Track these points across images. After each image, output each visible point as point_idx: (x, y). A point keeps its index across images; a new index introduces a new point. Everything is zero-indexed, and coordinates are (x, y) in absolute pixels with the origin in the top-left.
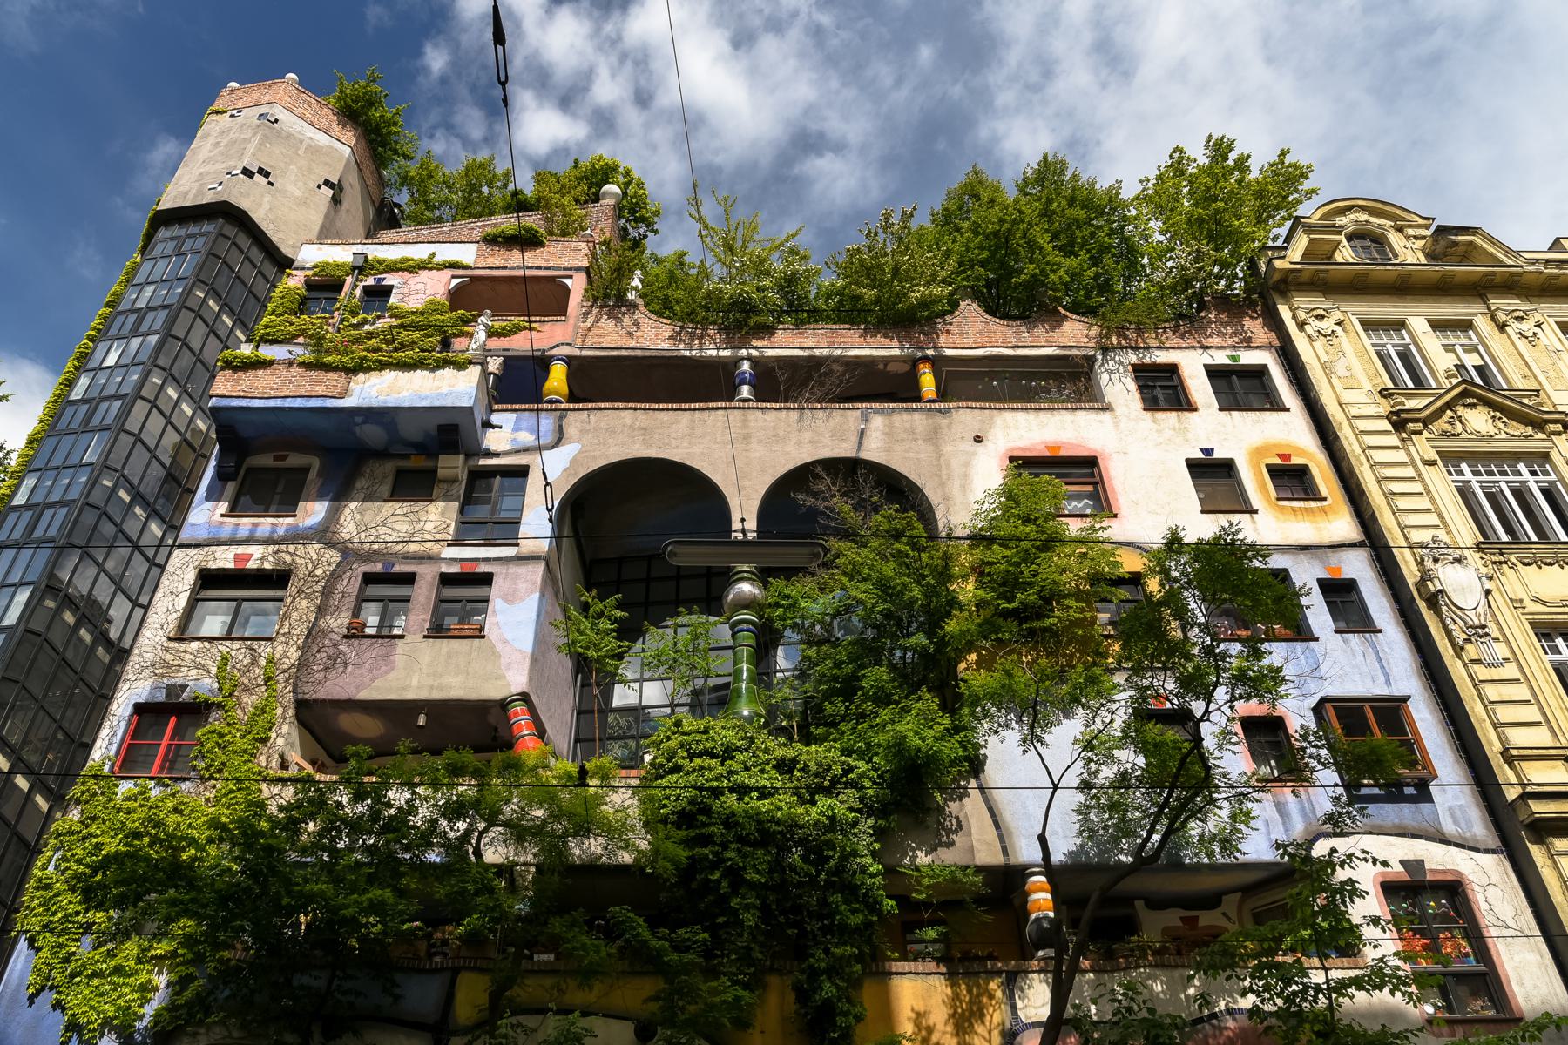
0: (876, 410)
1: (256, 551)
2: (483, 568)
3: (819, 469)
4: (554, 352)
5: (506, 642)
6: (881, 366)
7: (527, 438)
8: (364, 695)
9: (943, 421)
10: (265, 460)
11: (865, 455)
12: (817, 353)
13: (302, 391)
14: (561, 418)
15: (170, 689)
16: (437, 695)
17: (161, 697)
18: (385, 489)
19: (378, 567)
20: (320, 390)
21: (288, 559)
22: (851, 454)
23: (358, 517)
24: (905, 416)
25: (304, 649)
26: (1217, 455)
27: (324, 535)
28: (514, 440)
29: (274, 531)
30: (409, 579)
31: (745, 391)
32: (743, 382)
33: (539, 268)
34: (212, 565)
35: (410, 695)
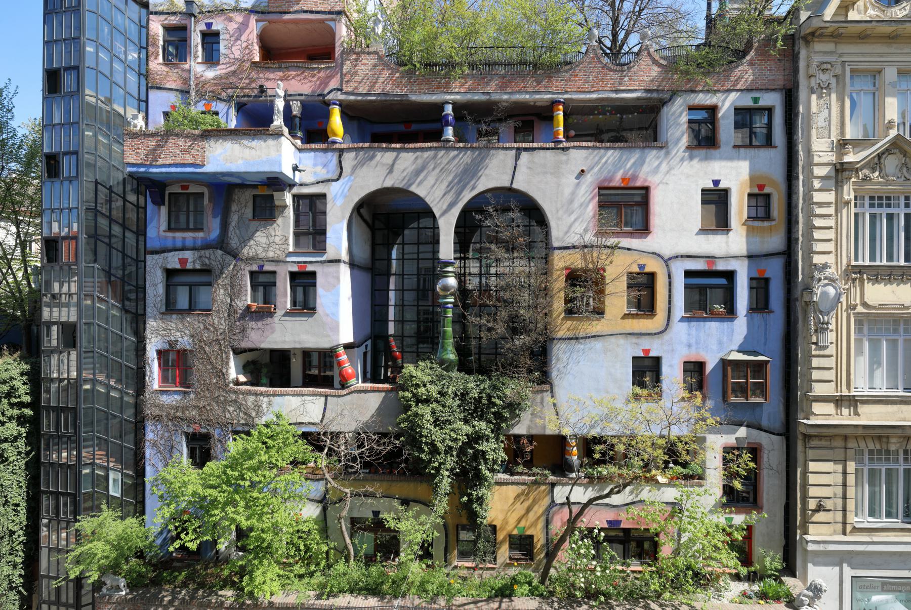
0: (526, 149)
2: (310, 268)
3: (489, 195)
4: (330, 97)
5: (328, 315)
7: (323, 174)
9: (562, 157)
11: (515, 186)
13: (178, 160)
14: (340, 156)
15: (170, 343)
17: (167, 347)
19: (255, 268)
21: (207, 261)
23: (238, 231)
28: (315, 173)
29: (195, 243)
32: (447, 124)
33: (312, 12)
34: (169, 267)
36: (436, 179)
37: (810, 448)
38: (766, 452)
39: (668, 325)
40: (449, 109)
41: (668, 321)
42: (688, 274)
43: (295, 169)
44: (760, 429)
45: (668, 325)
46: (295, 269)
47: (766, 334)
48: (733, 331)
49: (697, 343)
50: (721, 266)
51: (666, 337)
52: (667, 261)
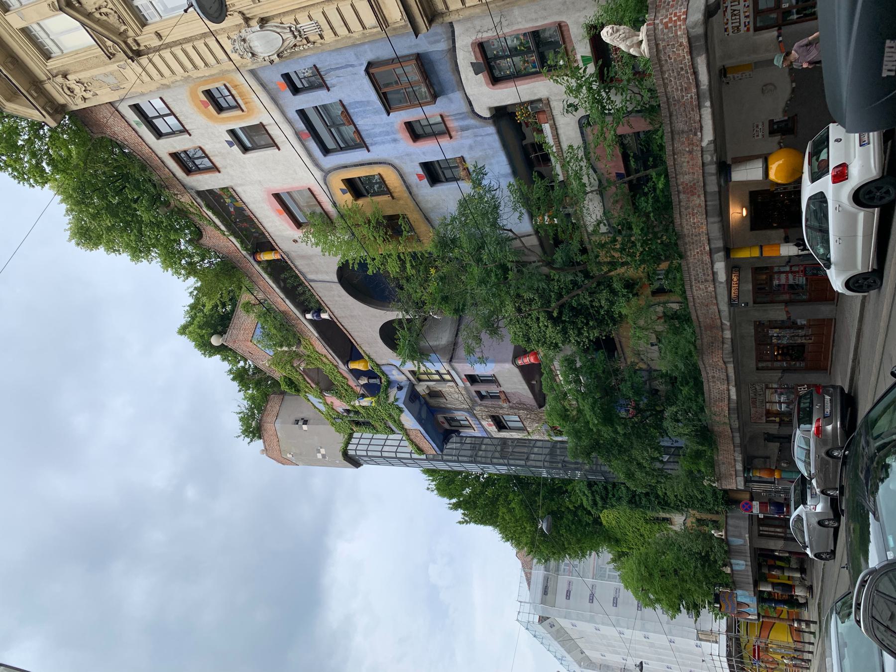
1: (484, 423)
6: (269, 269)
8: (531, 396)
10: (446, 426)
11: (336, 280)
12: (283, 296)
16: (523, 382)
18: (443, 400)
20: (420, 435)
22: (339, 285)
24: (300, 267)
25: (519, 410)
26: (230, 139)
27: (470, 411)
30: (478, 393)
31: (324, 316)
35: (526, 387)
36: (363, 322)
37: (447, 8)
38: (480, 35)
39: (384, 163)
40: (309, 316)
41: (380, 163)
42: (326, 151)
43: (400, 388)
44: (453, 49)
45: (384, 163)
46: (468, 384)
47: (342, 68)
48: (358, 102)
49: (387, 133)
50: (301, 126)
51: (396, 162)
52: (326, 173)
